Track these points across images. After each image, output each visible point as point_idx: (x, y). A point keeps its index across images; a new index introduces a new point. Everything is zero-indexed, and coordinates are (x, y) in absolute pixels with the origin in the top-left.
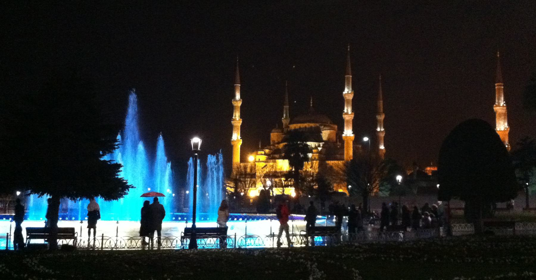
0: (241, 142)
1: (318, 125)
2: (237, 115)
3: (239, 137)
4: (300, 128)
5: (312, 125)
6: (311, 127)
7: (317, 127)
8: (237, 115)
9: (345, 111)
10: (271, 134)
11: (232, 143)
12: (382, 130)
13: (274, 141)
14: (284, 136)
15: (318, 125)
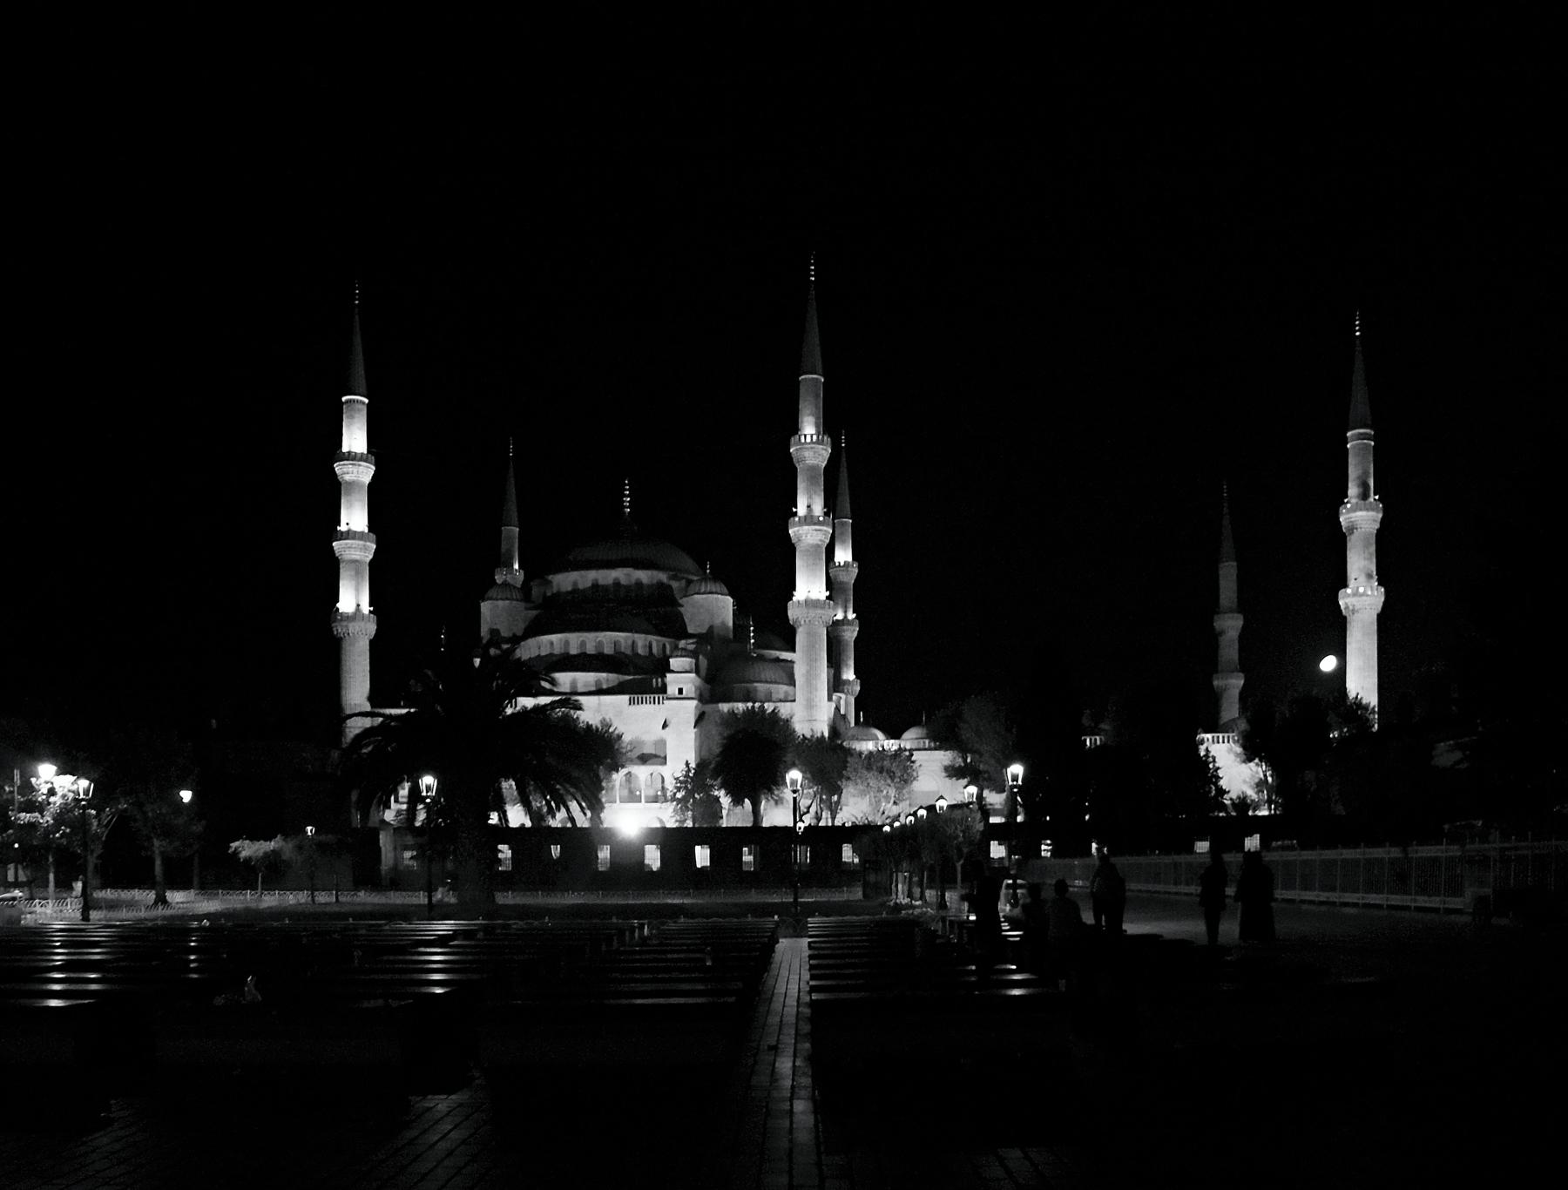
0: (371, 628)
1: (662, 577)
2: (354, 516)
3: (366, 608)
4: (595, 586)
5: (644, 576)
6: (639, 584)
7: (660, 585)
8: (354, 516)
9: (801, 510)
10: (485, 607)
11: (339, 629)
12: (851, 616)
13: (494, 632)
14: (535, 612)
15: (662, 577)
